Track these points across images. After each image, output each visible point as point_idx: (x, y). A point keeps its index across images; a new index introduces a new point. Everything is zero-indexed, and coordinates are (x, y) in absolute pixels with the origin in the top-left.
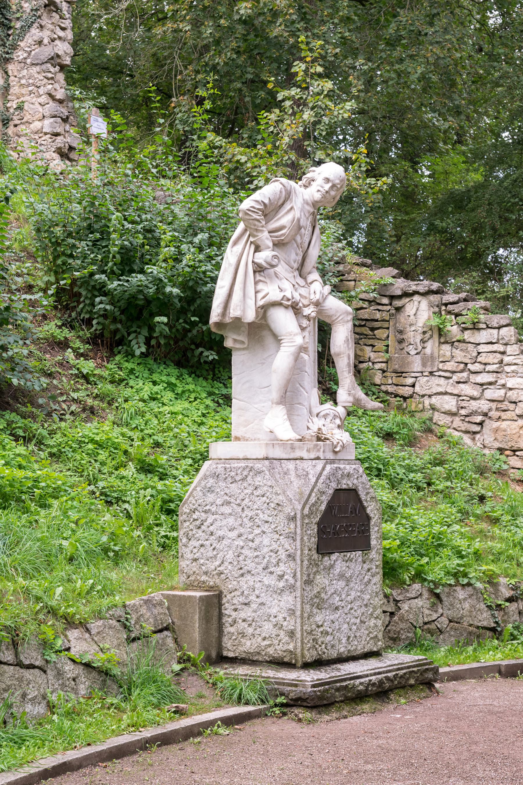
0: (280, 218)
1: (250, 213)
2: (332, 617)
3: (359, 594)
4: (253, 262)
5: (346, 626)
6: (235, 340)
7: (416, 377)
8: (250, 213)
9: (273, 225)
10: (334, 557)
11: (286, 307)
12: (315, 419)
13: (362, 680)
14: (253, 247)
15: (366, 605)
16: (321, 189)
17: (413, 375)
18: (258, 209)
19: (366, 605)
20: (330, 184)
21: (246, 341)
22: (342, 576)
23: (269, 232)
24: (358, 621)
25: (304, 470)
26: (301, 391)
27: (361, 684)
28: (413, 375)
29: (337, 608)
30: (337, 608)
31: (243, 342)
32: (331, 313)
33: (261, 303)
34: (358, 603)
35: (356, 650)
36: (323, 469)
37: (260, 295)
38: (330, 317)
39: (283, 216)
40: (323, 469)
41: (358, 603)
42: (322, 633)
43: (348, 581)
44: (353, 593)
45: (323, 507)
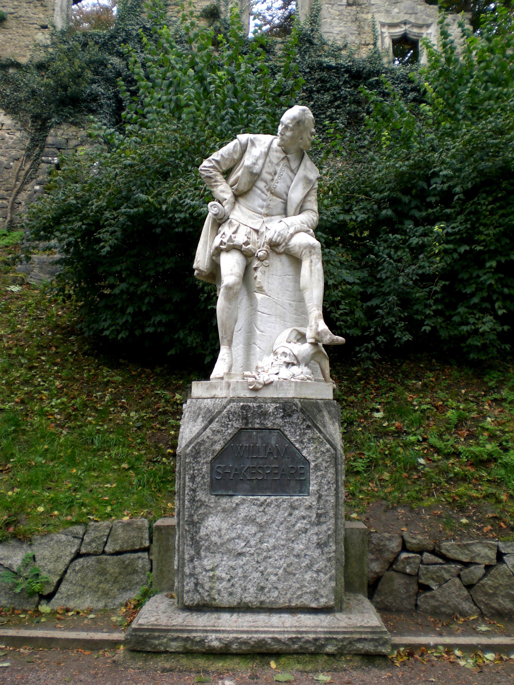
2: (232, 563)
3: (283, 543)
5: (258, 574)
9: (232, 179)
10: (237, 499)
11: (227, 251)
13: (221, 636)
15: (298, 556)
18: (210, 167)
19: (298, 556)
22: (249, 520)
24: (281, 571)
26: (255, 331)
27: (220, 640)
29: (240, 554)
30: (240, 554)
32: (297, 249)
34: (284, 552)
35: (272, 602)
41: (284, 552)
42: (211, 578)
43: (261, 527)
44: (272, 541)
45: (218, 447)
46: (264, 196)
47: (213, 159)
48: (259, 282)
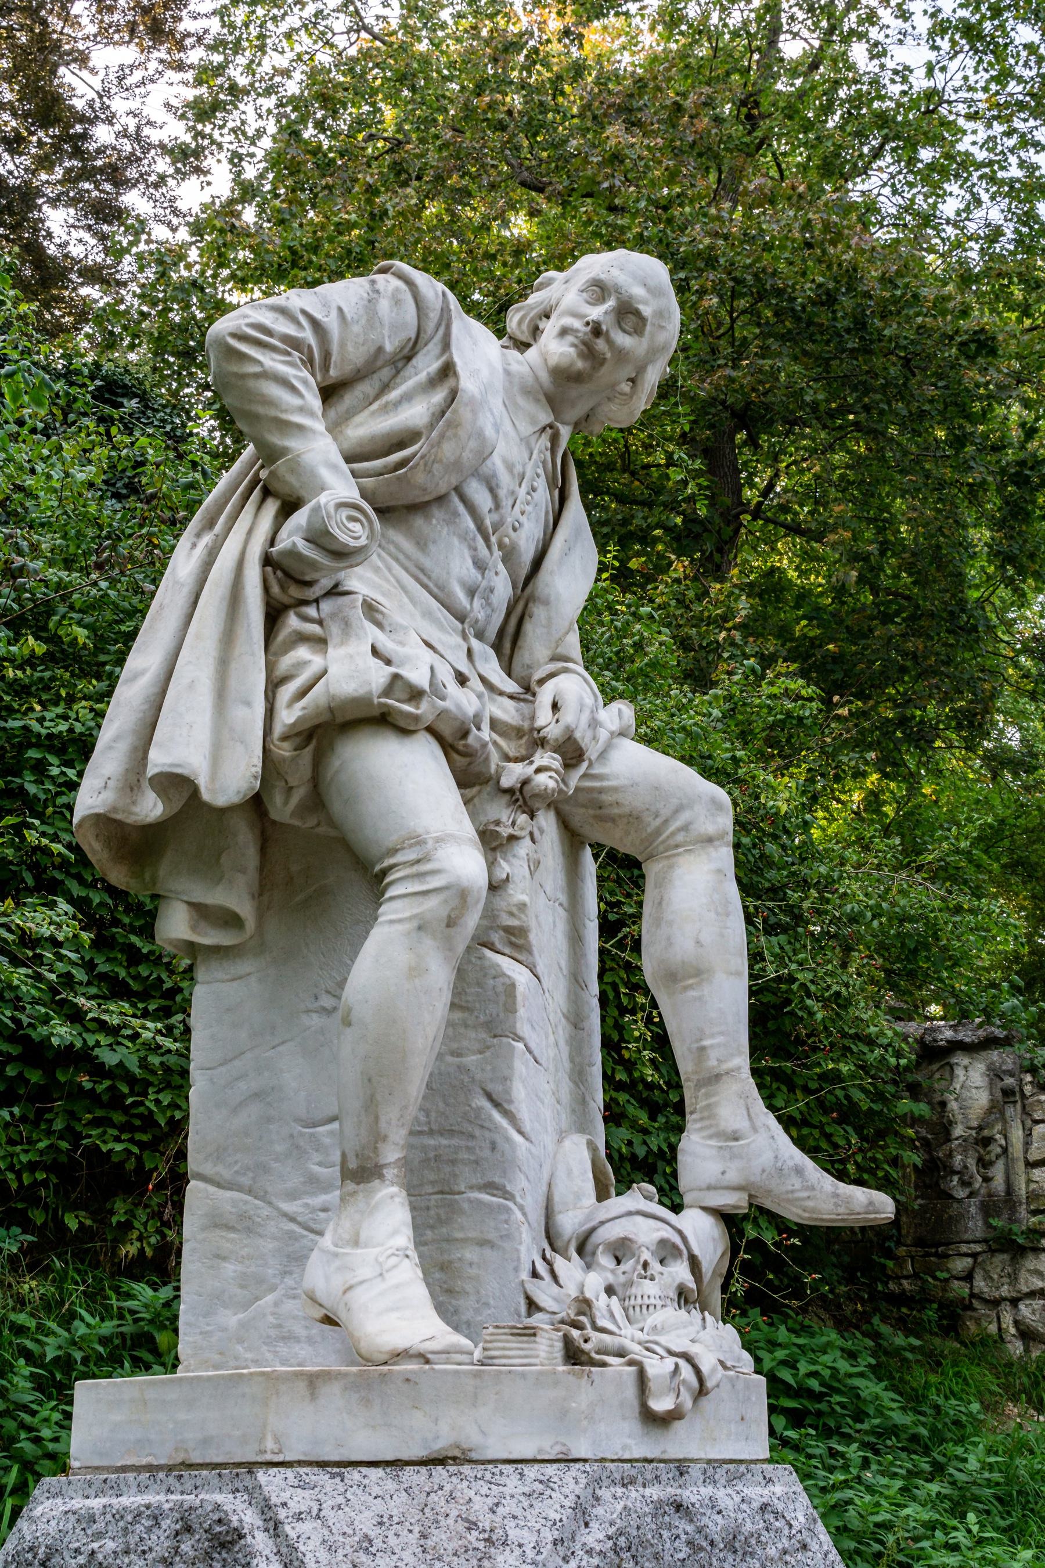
0: (397, 404)
1: (243, 347)
4: (267, 561)
6: (201, 912)
7: (974, 1255)
8: (243, 347)
12: (569, 1268)
14: (271, 507)
16: (577, 324)
17: (964, 1248)
20: (611, 303)
21: (245, 909)
23: (349, 459)
25: (472, 1525)
28: (964, 1248)
31: (230, 920)
32: (632, 801)
33: (287, 716)
36: (582, 1514)
37: (286, 692)
38: (634, 818)
39: (407, 398)
40: (582, 1514)
46: (483, 550)
47: (304, 312)
48: (522, 906)
